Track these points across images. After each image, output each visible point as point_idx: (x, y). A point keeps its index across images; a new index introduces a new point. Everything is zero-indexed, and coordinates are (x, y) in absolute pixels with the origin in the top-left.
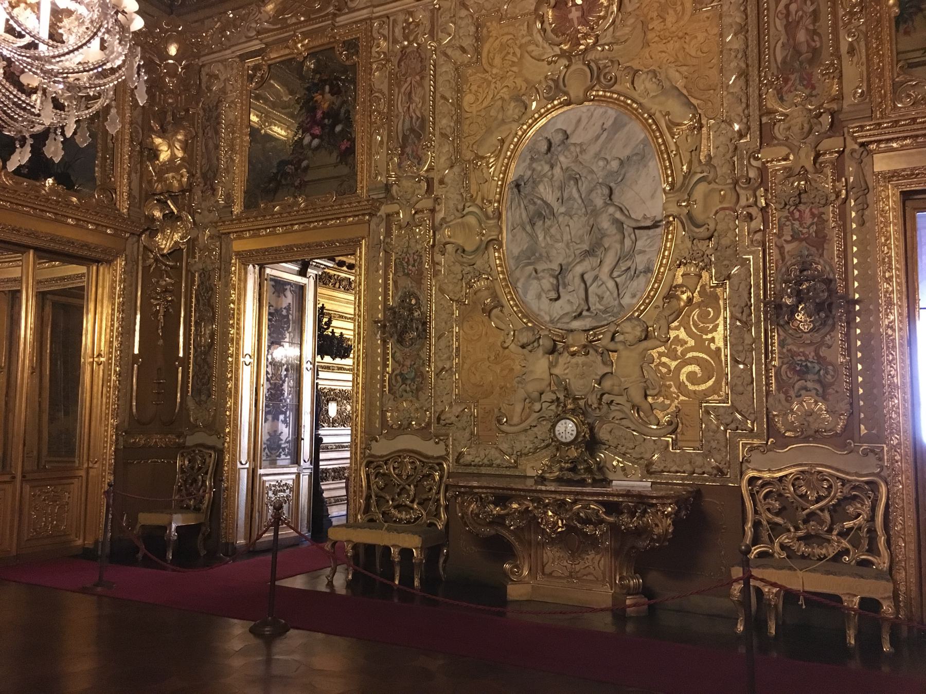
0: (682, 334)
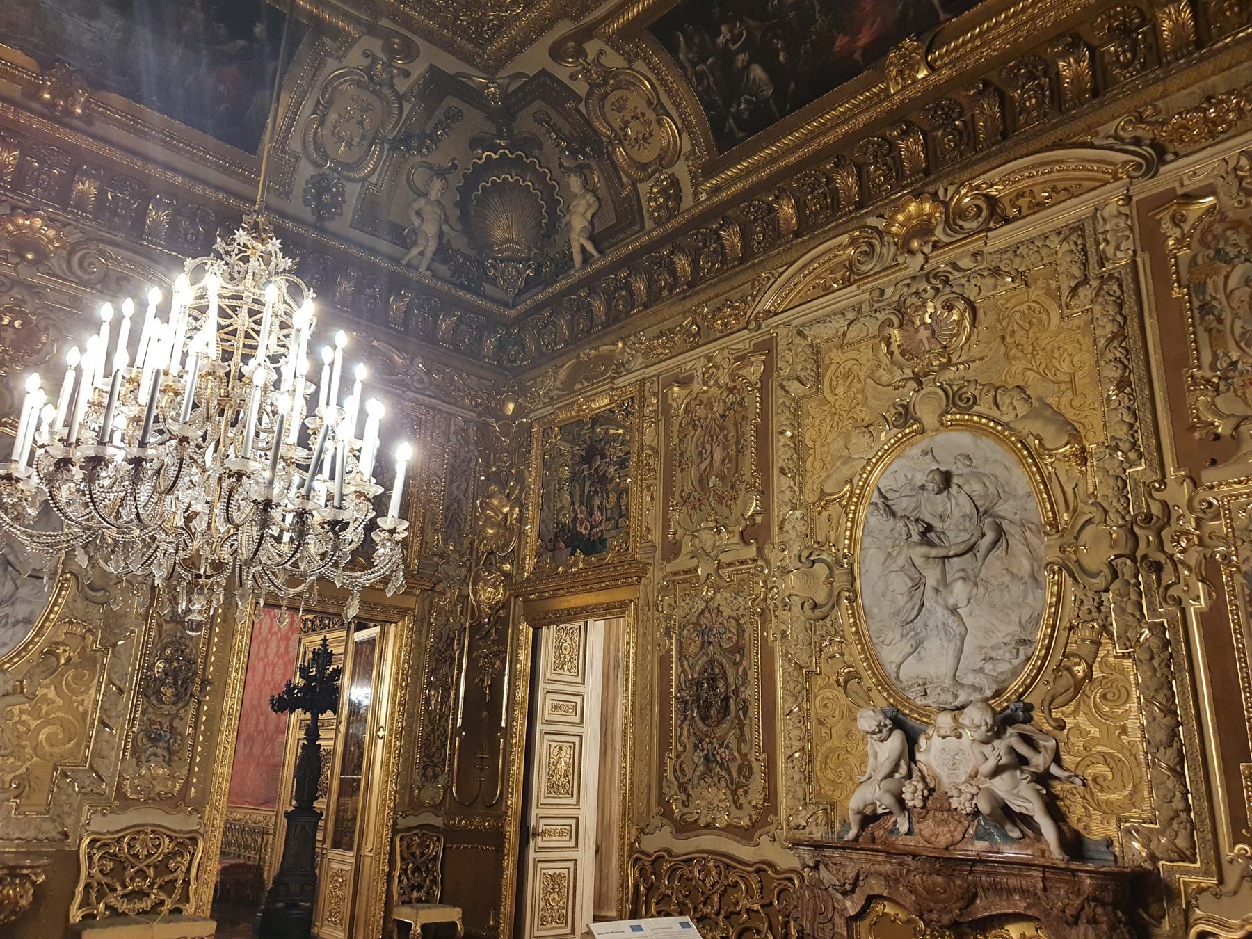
0: (51, 692)
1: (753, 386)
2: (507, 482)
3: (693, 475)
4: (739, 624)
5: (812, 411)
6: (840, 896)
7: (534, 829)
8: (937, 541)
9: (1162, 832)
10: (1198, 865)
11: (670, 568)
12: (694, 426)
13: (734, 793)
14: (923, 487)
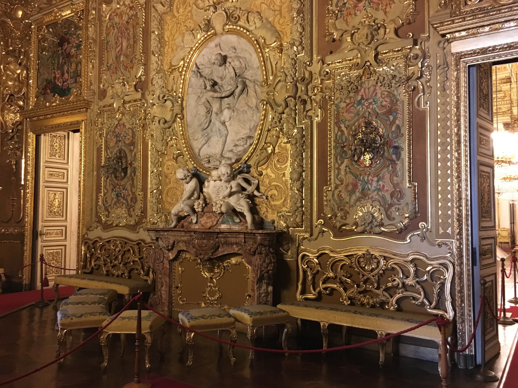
1: (142, 6)
2: (20, 57)
3: (113, 54)
4: (133, 132)
5: (168, 21)
6: (167, 252)
7: (41, 232)
8: (218, 90)
9: (291, 216)
10: (303, 228)
11: (101, 104)
12: (114, 27)
13: (129, 210)
14: (214, 63)
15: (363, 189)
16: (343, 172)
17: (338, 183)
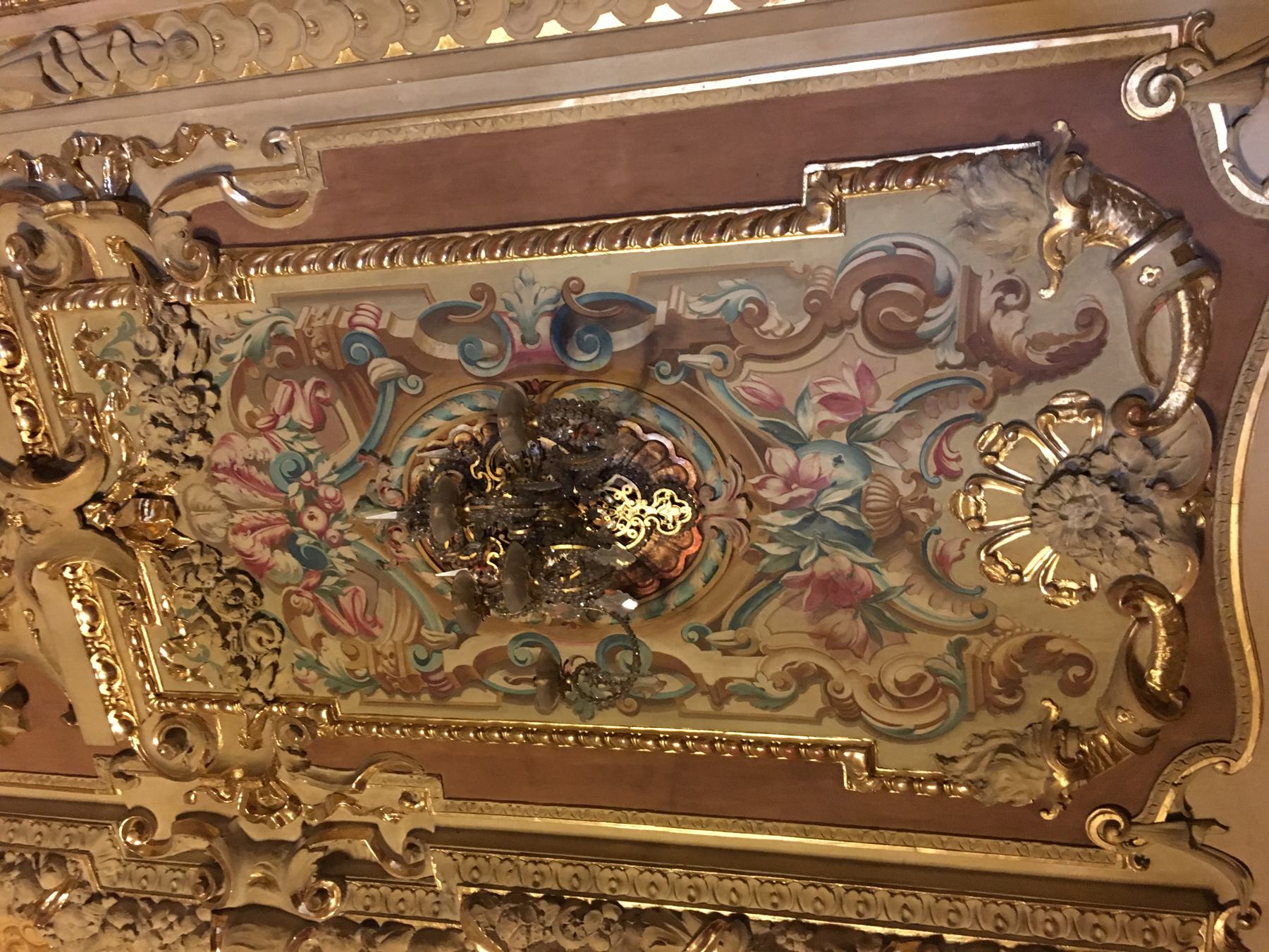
15: (859, 539)
16: (743, 669)
17: (813, 699)
